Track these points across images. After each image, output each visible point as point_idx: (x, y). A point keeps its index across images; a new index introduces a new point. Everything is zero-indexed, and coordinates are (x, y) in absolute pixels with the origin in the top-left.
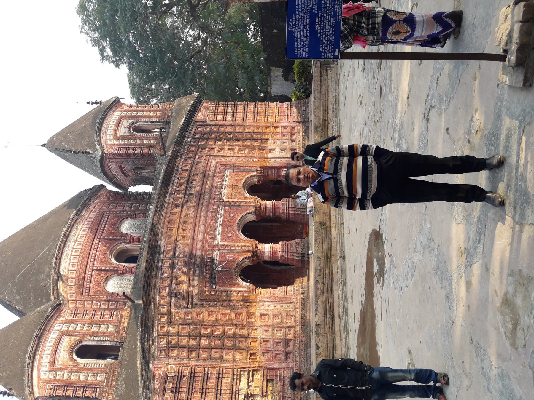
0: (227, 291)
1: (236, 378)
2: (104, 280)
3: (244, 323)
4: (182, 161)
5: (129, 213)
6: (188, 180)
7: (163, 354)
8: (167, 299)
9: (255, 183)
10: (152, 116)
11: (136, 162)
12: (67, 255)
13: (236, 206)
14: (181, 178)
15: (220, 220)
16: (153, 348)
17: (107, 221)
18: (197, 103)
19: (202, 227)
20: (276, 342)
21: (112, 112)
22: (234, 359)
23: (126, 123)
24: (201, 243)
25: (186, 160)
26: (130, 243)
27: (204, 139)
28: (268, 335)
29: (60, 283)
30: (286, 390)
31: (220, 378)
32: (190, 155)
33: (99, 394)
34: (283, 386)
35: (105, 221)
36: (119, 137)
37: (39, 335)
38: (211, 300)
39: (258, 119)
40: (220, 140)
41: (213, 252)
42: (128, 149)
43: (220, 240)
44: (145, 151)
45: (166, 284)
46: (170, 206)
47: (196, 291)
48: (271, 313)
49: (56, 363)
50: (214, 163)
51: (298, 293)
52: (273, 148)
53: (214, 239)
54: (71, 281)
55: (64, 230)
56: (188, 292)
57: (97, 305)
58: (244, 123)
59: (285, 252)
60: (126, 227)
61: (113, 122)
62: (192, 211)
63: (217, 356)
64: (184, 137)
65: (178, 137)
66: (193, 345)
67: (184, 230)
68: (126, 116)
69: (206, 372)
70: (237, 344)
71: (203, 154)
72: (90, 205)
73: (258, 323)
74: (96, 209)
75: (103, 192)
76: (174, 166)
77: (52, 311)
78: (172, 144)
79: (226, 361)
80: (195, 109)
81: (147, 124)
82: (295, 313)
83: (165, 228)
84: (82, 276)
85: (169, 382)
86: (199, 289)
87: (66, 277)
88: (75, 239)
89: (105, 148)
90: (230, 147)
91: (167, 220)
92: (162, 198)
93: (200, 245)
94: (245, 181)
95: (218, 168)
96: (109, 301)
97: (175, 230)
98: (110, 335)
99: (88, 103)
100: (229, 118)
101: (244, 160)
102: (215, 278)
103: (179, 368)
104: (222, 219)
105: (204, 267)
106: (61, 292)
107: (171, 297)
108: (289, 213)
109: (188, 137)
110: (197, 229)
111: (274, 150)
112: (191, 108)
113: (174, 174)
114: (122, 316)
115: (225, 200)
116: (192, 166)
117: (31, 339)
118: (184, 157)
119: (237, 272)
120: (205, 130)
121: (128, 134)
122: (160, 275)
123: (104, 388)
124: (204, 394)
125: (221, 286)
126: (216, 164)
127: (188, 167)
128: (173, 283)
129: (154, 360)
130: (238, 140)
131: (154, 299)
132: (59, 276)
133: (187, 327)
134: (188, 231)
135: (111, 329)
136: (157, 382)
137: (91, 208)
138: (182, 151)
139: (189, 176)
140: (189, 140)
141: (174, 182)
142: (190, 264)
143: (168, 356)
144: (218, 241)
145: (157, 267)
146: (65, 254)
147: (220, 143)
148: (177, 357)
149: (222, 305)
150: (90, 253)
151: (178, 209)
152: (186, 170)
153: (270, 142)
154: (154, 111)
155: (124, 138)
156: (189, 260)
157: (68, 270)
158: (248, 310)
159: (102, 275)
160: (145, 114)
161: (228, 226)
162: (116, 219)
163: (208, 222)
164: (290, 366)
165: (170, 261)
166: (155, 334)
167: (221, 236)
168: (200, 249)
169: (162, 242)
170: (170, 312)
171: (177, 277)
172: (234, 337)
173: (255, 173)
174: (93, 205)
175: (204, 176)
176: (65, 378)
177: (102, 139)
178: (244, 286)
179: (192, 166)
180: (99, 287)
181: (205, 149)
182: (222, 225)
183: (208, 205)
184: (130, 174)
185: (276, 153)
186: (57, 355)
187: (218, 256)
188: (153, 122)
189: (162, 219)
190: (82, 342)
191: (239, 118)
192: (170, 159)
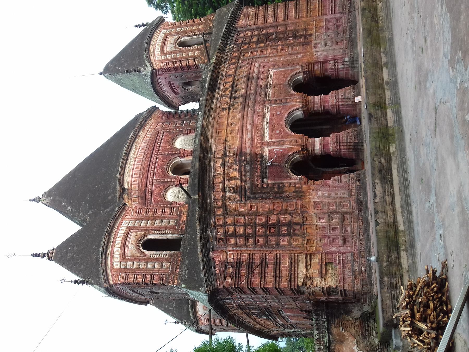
0: (279, 184)
3: (298, 211)
4: (226, 67)
5: (181, 130)
7: (222, 243)
9: (300, 81)
10: (195, 29)
11: (184, 76)
12: (130, 172)
14: (226, 83)
15: (267, 119)
18: (237, 9)
19: (249, 127)
20: (333, 228)
21: (158, 31)
22: (290, 245)
23: (171, 40)
24: (250, 141)
25: (230, 66)
26: (184, 156)
27: (245, 44)
28: (324, 222)
29: (125, 196)
30: (346, 272)
31: (277, 263)
33: (165, 280)
34: (343, 268)
35: (160, 139)
37: (109, 231)
38: (264, 193)
39: (300, 16)
40: (262, 42)
41: (262, 149)
42: (174, 63)
43: (268, 137)
44: (191, 62)
45: (220, 181)
46: (218, 110)
47: (248, 185)
48: (325, 201)
49: (126, 254)
50: (257, 65)
53: (262, 137)
54: (134, 194)
55: (125, 149)
56: (241, 187)
58: (286, 23)
59: (337, 143)
61: (160, 40)
62: (238, 113)
63: (273, 243)
64: (226, 44)
66: (250, 234)
67: (232, 131)
68: (171, 33)
69: (264, 257)
70: (292, 232)
75: (157, 113)
76: (218, 72)
77: (119, 209)
78: (215, 52)
79: (283, 247)
80: (235, 17)
81: (192, 37)
83: (214, 131)
85: (229, 268)
86: (251, 183)
87: (130, 191)
88: (135, 157)
89: (154, 64)
90: (273, 47)
91: (215, 123)
92: (209, 103)
93: (248, 143)
94: (290, 79)
97: (224, 132)
98: (171, 228)
100: (270, 20)
102: (266, 173)
103: (237, 255)
104: (268, 117)
107: (225, 192)
108: (339, 105)
111: (319, 44)
112: (232, 15)
113: (219, 80)
114: (181, 211)
116: (236, 70)
117: (102, 235)
118: (227, 63)
119: (288, 165)
120: (246, 35)
121: (175, 49)
122: (213, 174)
123: (169, 275)
124: (263, 278)
127: (232, 72)
128: (226, 179)
129: (213, 249)
130: (280, 39)
131: (210, 195)
132: (124, 189)
133: (242, 218)
134: (237, 131)
135: (172, 223)
136: (218, 268)
138: (225, 57)
139: (234, 80)
140: (232, 46)
141: (219, 88)
142: (240, 161)
143: (226, 245)
144: (267, 137)
146: (127, 170)
147: (262, 45)
148: (235, 244)
151: (225, 112)
152: (231, 75)
153: (313, 37)
154: (196, 25)
155: (171, 53)
156: (239, 158)
157: (131, 185)
158: (301, 200)
160: (189, 28)
164: (349, 249)
165: (221, 160)
166: (213, 225)
167: (269, 134)
169: (213, 143)
171: (229, 174)
172: (289, 224)
173: (300, 70)
174: (148, 126)
175: (248, 79)
176: (134, 268)
177: (151, 57)
178: (295, 178)
179: (236, 70)
181: (248, 53)
182: (269, 123)
183: (254, 105)
184: (179, 91)
185: (322, 46)
186: (126, 248)
187: (267, 152)
188: (196, 35)
189: (211, 122)
190: (147, 236)
191: (281, 18)
192: (214, 66)
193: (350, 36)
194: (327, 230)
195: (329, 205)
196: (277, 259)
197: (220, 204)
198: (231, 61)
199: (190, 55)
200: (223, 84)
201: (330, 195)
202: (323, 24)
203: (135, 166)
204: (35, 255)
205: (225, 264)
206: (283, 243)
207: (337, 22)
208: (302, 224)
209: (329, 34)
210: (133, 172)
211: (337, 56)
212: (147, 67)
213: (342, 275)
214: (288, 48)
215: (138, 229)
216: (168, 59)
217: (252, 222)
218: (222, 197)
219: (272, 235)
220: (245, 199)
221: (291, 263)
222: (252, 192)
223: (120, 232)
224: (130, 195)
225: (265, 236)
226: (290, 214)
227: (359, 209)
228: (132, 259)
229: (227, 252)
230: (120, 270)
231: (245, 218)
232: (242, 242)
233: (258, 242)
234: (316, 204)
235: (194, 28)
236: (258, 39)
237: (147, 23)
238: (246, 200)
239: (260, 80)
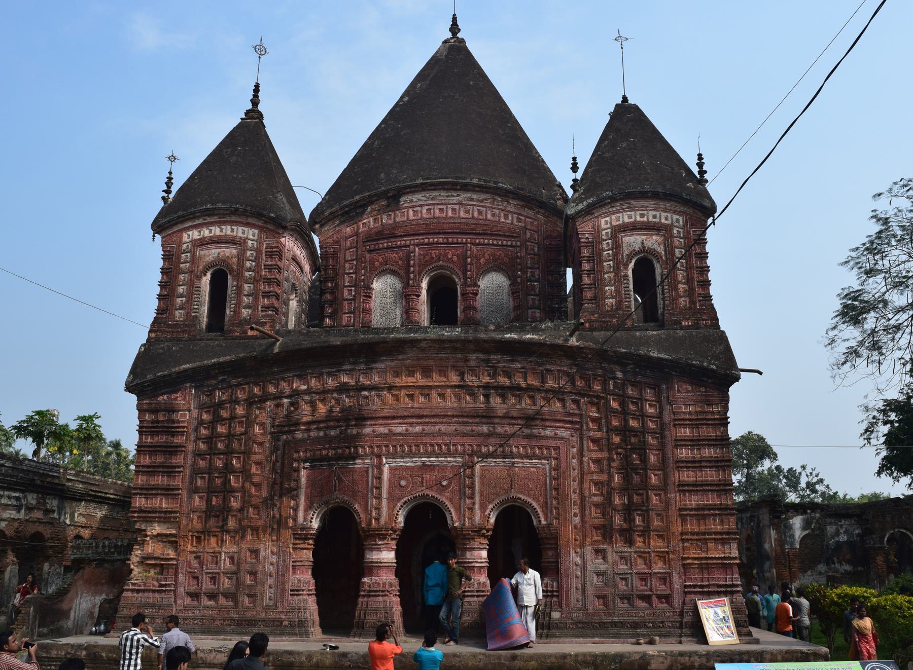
0: (298, 488)
1: (166, 517)
3: (245, 523)
5: (519, 280)
6: (518, 388)
8: (288, 391)
10: (676, 288)
12: (432, 199)
13: (465, 491)
14: (526, 373)
16: (214, 382)
17: (502, 245)
19: (418, 429)
21: (679, 208)
23: (653, 242)
24: (386, 431)
25: (567, 374)
26: (462, 295)
27: (622, 404)
29: (384, 203)
30: (146, 594)
32: (580, 383)
35: (500, 242)
36: (616, 237)
38: (283, 464)
42: (590, 260)
46: (461, 364)
47: (299, 435)
48: (260, 567)
50: (563, 433)
51: (291, 616)
52: (609, 558)
53: (394, 456)
55: (475, 181)
56: (298, 424)
57: (350, 269)
58: (671, 487)
59: (370, 591)
60: (492, 283)
65: (615, 352)
67: (411, 397)
68: (672, 236)
71: (584, 407)
72: (530, 208)
73: (244, 546)
74: (525, 222)
79: (190, 498)
82: (258, 609)
86: (303, 440)
90: (605, 462)
91: (431, 363)
92: (472, 346)
93: (383, 430)
95: (551, 443)
96: (355, 286)
98: (237, 312)
99: (700, 157)
101: (574, 497)
105: (339, 444)
106: (369, 209)
107: (289, 397)
109: (624, 372)
110: (414, 420)
111: (604, 559)
113: (531, 359)
115: (477, 468)
121: (626, 252)
125: (308, 477)
126: (562, 438)
127: (551, 383)
129: (196, 388)
130: (626, 478)
131: (287, 371)
135: (245, 312)
137: (527, 212)
139: (529, 388)
140: (619, 375)
141: (513, 361)
143: (201, 407)
145: (342, 364)
147: (616, 439)
149: (274, 483)
150: (440, 233)
152: (543, 381)
155: (617, 246)
157: (406, 207)
159: (400, 262)
160: (681, 275)
161: (422, 478)
162: (506, 260)
163: (426, 439)
164: (179, 602)
166: (234, 381)
168: (374, 431)
169: (388, 363)
170: (266, 400)
173: (543, 522)
174: (531, 213)
180: (381, 264)
181: (598, 411)
182: (424, 465)
185: (595, 564)
188: (663, 294)
193: (614, 624)
194: (212, 568)
195: (253, 573)
196: (173, 490)
197: (272, 389)
198: (581, 378)
199: (607, 288)
200: (523, 368)
201: (271, 576)
202: (659, 567)
203: (444, 207)
204: (257, 89)
205: (172, 410)
206: (197, 499)
207: (660, 597)
208: (223, 529)
209: (630, 581)
210: (433, 204)
211: (567, 596)
212: (577, 205)
213: (143, 588)
214: (602, 494)
215: (241, 257)
216: (600, 243)
217: (235, 445)
218: (281, 392)
219: (211, 480)
220: (274, 433)
221: (166, 512)
222: (286, 442)
223: (240, 228)
224: (387, 209)
225: (210, 470)
226: (241, 510)
227: (242, 621)
228: (193, 260)
229: (189, 411)
230: (181, 243)
231: (242, 434)
232: (204, 432)
233: (203, 459)
234: (255, 552)
235: (680, 286)
236: (632, 430)
237: (707, 181)
238: (271, 433)
239: (524, 442)
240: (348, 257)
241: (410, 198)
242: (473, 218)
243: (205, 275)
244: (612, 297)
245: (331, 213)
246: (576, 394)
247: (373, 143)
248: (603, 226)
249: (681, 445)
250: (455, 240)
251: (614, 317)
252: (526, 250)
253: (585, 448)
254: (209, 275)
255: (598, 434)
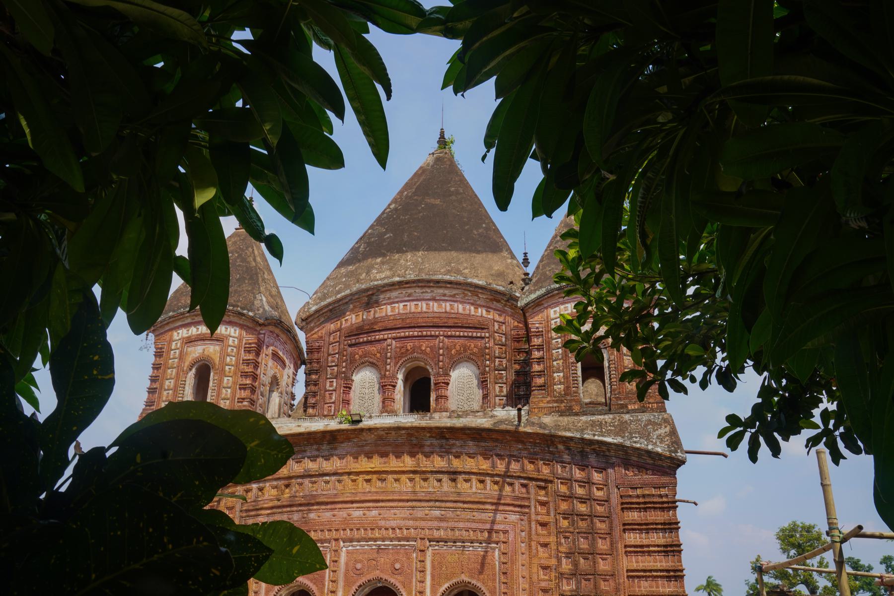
2: (371, 360)
5: (487, 369)
12: (409, 296)
26: (436, 384)
35: (470, 334)
57: (333, 362)
67: (368, 481)
71: (532, 491)
84: (377, 327)
115: (429, 553)
134: (367, 490)
146: (410, 291)
147: (565, 523)
150: (414, 327)
159: (378, 355)
162: (475, 350)
180: (361, 357)
186: (199, 343)
198: (530, 462)
199: (555, 375)
228: (181, 357)
240: (331, 351)
241: (388, 295)
242: (446, 312)
243: (190, 370)
244: (561, 383)
245: (317, 311)
246: (525, 478)
247: (359, 247)
248: (552, 315)
249: (628, 529)
250: (429, 333)
251: (562, 402)
252: (495, 340)
253: (533, 532)
254: (194, 370)
255: (545, 519)
